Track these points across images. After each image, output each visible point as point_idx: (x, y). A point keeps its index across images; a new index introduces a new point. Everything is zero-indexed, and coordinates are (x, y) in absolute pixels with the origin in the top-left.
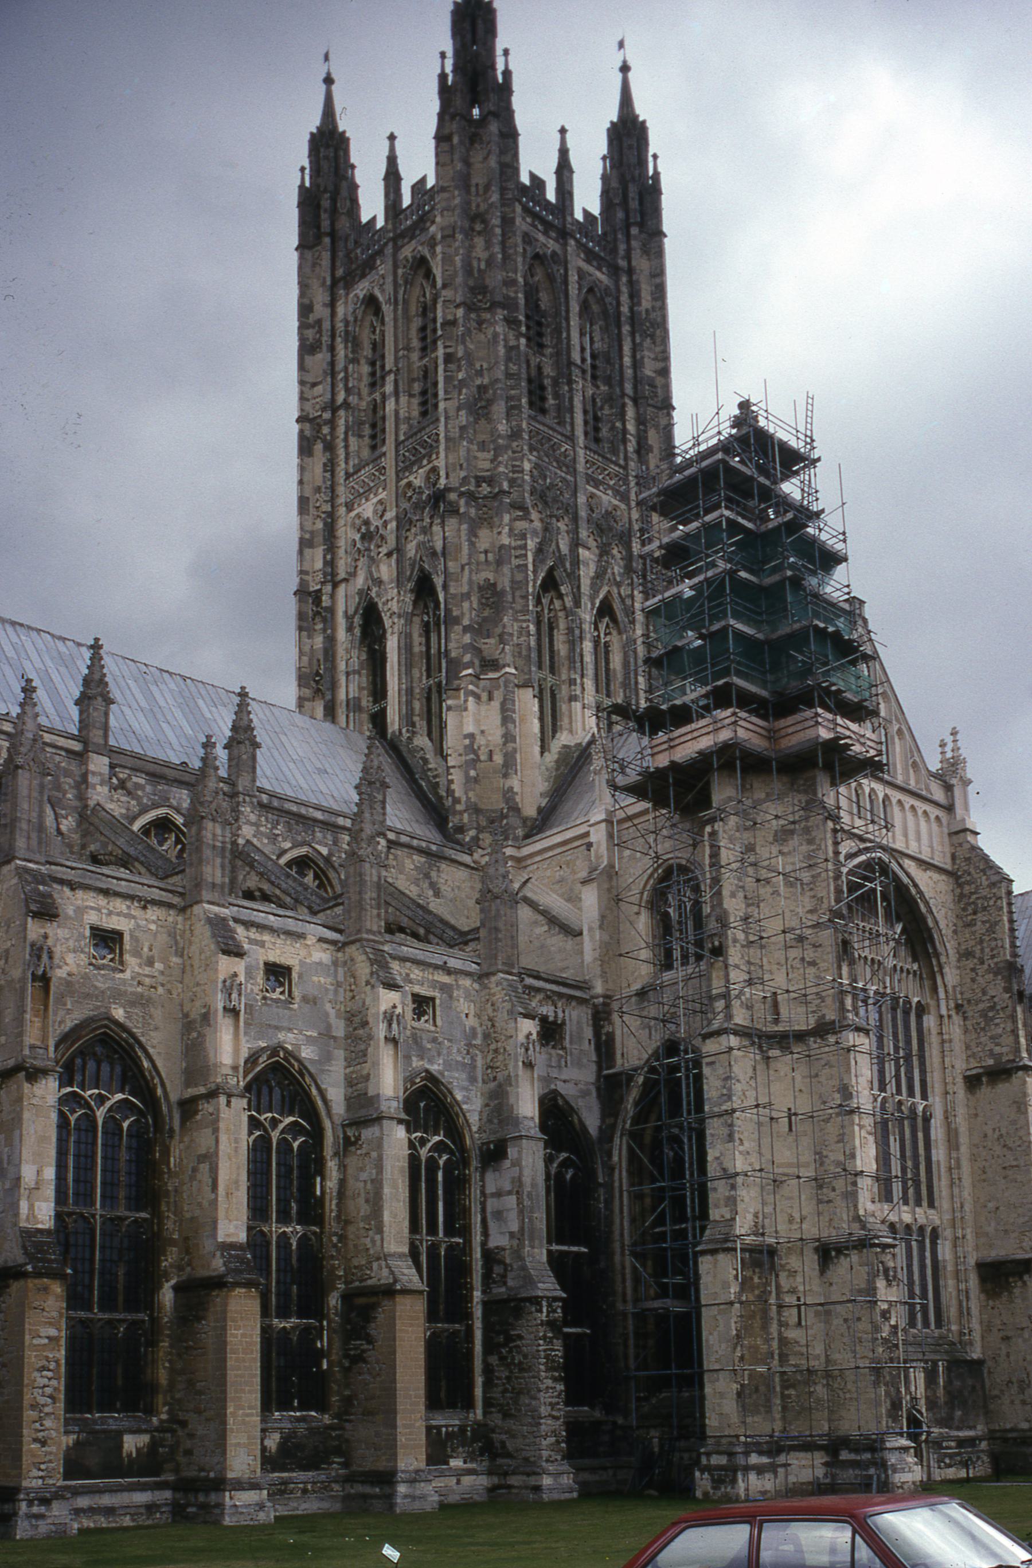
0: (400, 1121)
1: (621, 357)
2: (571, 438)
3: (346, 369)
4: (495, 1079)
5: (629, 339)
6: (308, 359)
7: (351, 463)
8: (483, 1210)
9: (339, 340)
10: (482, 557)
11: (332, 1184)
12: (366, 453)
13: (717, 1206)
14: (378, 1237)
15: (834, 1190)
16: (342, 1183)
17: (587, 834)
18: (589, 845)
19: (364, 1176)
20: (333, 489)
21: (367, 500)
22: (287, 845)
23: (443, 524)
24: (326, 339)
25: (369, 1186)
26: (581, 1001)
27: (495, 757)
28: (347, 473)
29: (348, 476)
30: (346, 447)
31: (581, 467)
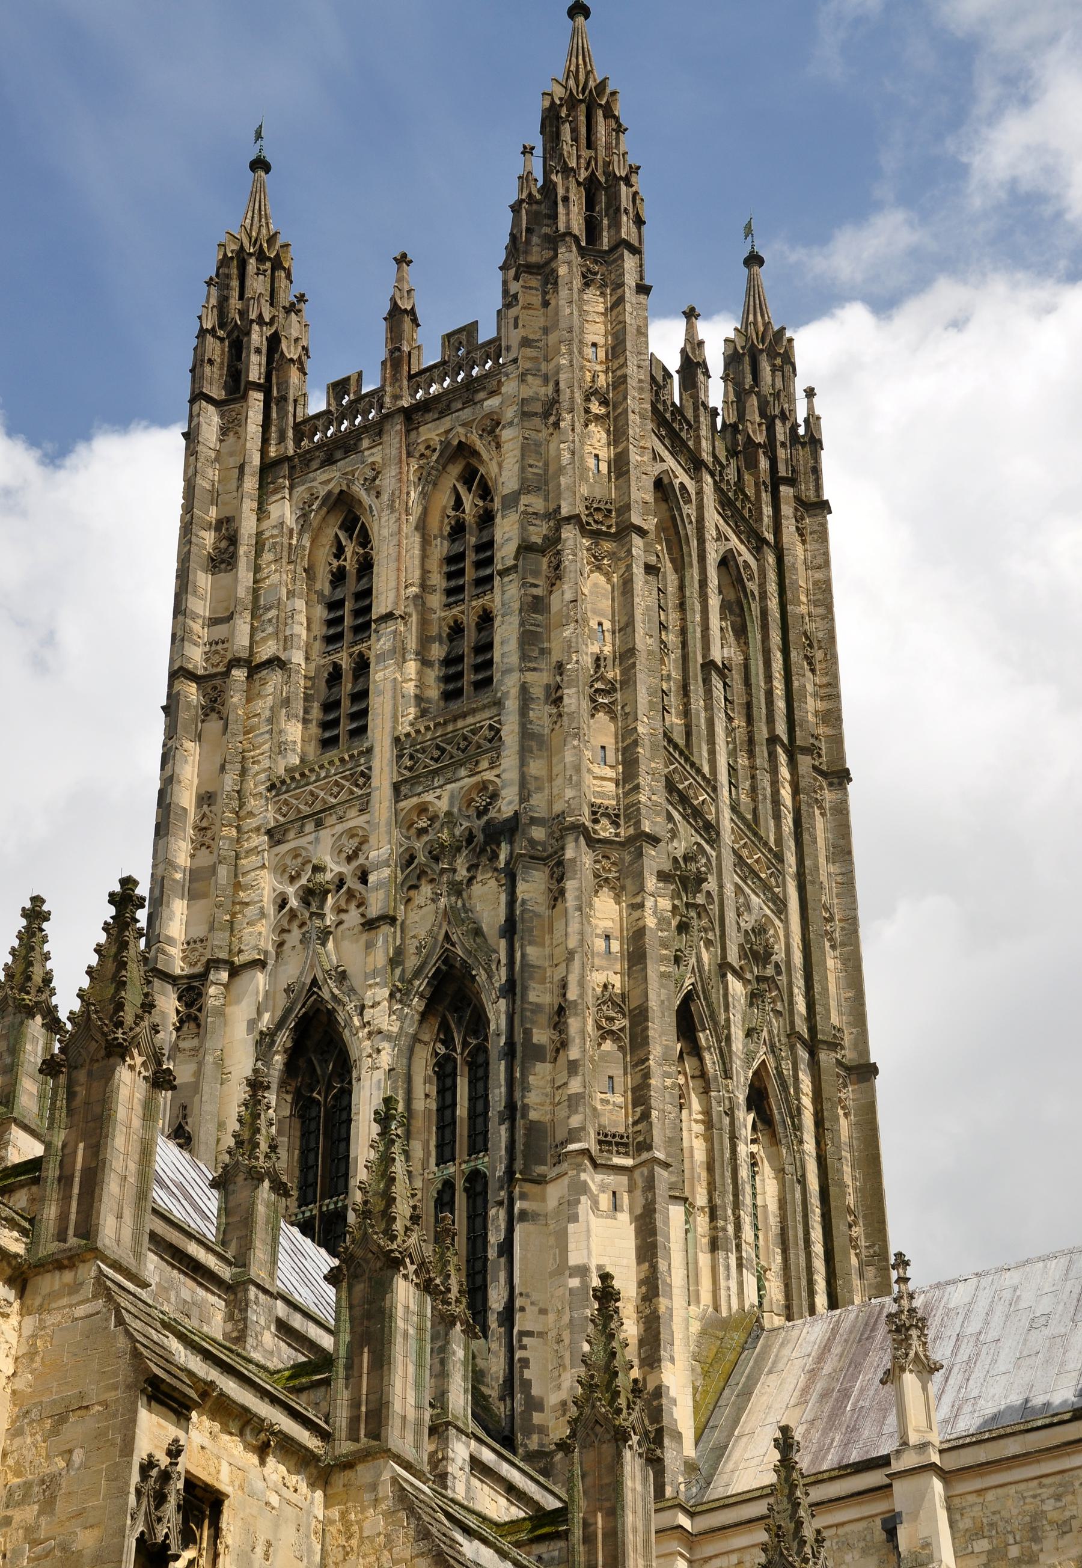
1: (769, 678)
5: (779, 655)
9: (268, 556)
10: (600, 944)
21: (319, 824)
23: (510, 879)
31: (727, 836)
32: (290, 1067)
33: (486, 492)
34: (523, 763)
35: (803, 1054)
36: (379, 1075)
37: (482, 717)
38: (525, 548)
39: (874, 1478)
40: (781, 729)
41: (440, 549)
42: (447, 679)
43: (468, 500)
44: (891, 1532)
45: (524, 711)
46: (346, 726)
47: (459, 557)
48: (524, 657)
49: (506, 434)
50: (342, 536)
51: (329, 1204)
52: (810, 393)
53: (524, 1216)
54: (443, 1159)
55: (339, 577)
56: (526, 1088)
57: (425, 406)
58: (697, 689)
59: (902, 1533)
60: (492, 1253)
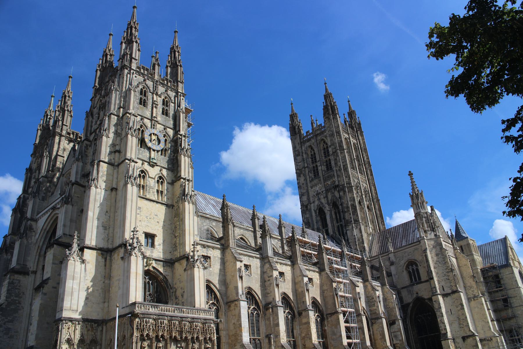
0: (384, 318)
2: (357, 173)
3: (306, 160)
4: (389, 308)
6: (297, 157)
7: (310, 179)
8: (392, 336)
9: (304, 154)
11: (371, 332)
12: (313, 177)
13: (442, 330)
14: (385, 343)
15: (463, 325)
16: (373, 332)
18: (389, 258)
19: (378, 330)
21: (316, 186)
24: (301, 154)
25: (380, 332)
26: (396, 290)
28: (310, 181)
29: (310, 182)
30: (309, 175)
33: (327, 144)
34: (338, 179)
36: (329, 215)
37: (332, 173)
38: (333, 153)
39: (387, 254)
41: (323, 151)
42: (326, 167)
43: (325, 145)
45: (337, 173)
46: (316, 173)
47: (325, 152)
48: (336, 166)
49: (328, 138)
52: (358, 118)
53: (348, 230)
54: (337, 222)
55: (312, 155)
56: (345, 216)
57: (318, 134)
58: (353, 162)
60: (345, 233)
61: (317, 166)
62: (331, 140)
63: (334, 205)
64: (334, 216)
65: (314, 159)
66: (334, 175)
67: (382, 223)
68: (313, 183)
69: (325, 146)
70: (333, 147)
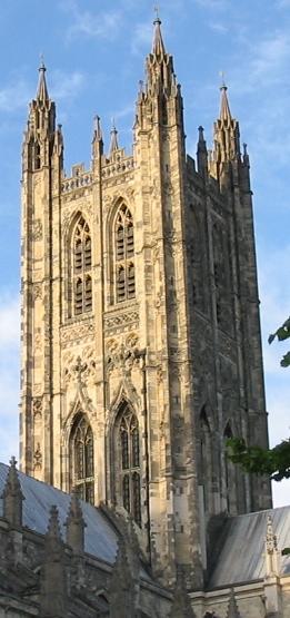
1: (231, 269)
2: (211, 321)
17: (262, 589)
20: (51, 330)
22: (94, 588)
24: (45, 233)
27: (185, 531)
30: (61, 306)
31: (217, 341)
32: (73, 431)
33: (130, 216)
34: (148, 332)
35: (243, 411)
38: (145, 247)
39: (260, 585)
40: (235, 289)
44: (264, 602)
47: (122, 241)
48: (147, 290)
49: (136, 198)
50: (80, 227)
51: (88, 480)
52: (245, 146)
55: (79, 242)
59: (267, 603)
60: (142, 504)
61: (89, 279)
62: (146, 206)
63: (123, 410)
64: (118, 448)
65: (84, 260)
66: (137, 317)
67: (265, 486)
68: (67, 331)
69: (123, 220)
70: (149, 229)
